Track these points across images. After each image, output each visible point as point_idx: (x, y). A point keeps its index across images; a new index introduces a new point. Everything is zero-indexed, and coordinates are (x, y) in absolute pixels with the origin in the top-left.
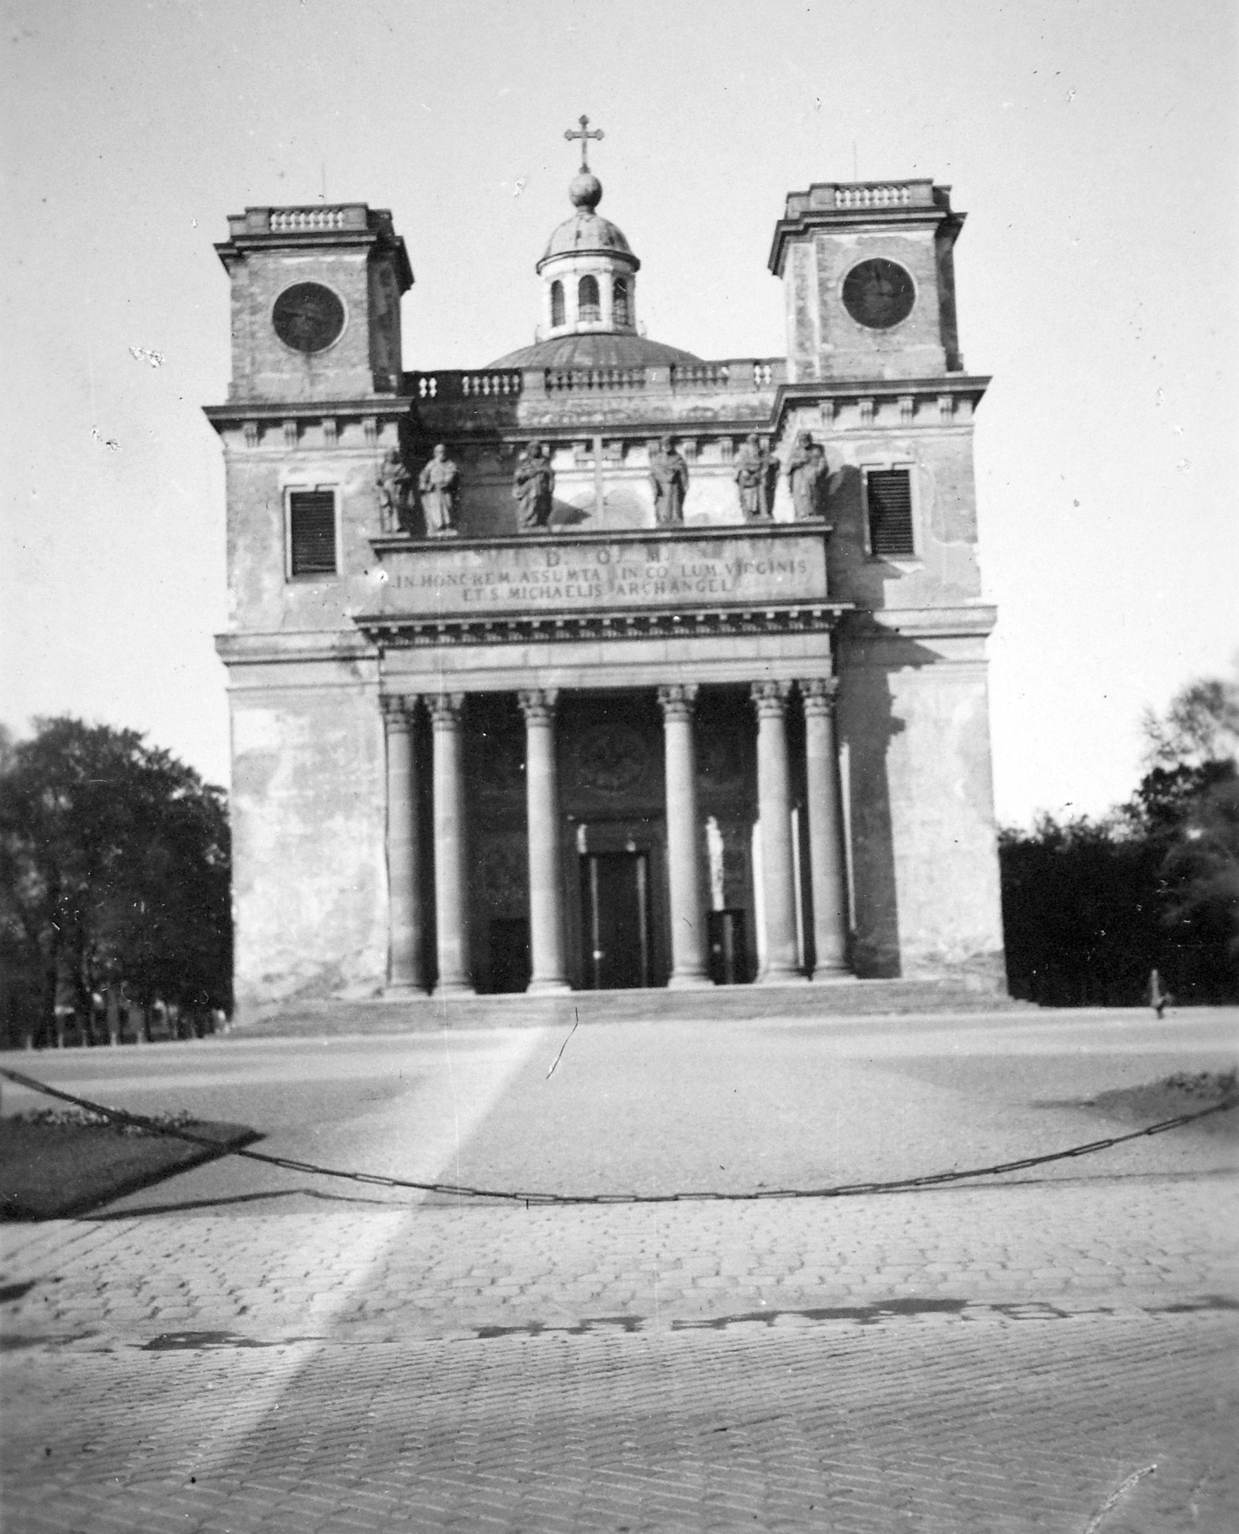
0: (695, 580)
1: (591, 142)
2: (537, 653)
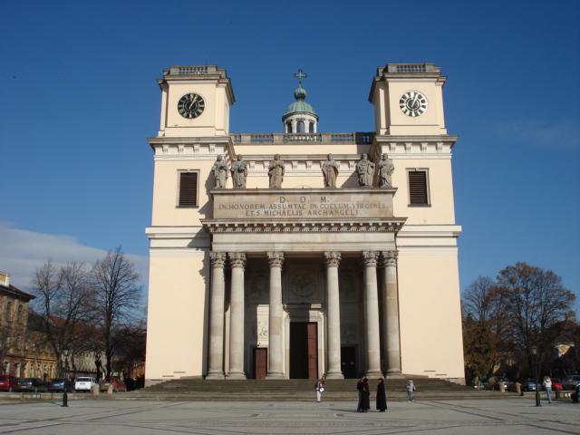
2: (274, 237)
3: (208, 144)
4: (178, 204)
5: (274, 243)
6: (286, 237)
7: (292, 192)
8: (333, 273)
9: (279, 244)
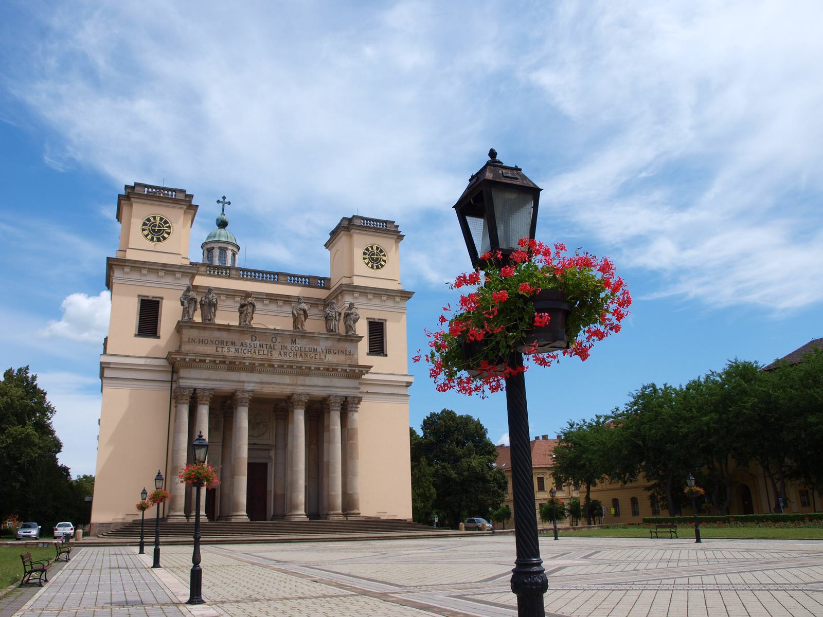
1: (226, 205)
2: (243, 376)
3: (175, 271)
4: (137, 333)
5: (244, 382)
6: (256, 377)
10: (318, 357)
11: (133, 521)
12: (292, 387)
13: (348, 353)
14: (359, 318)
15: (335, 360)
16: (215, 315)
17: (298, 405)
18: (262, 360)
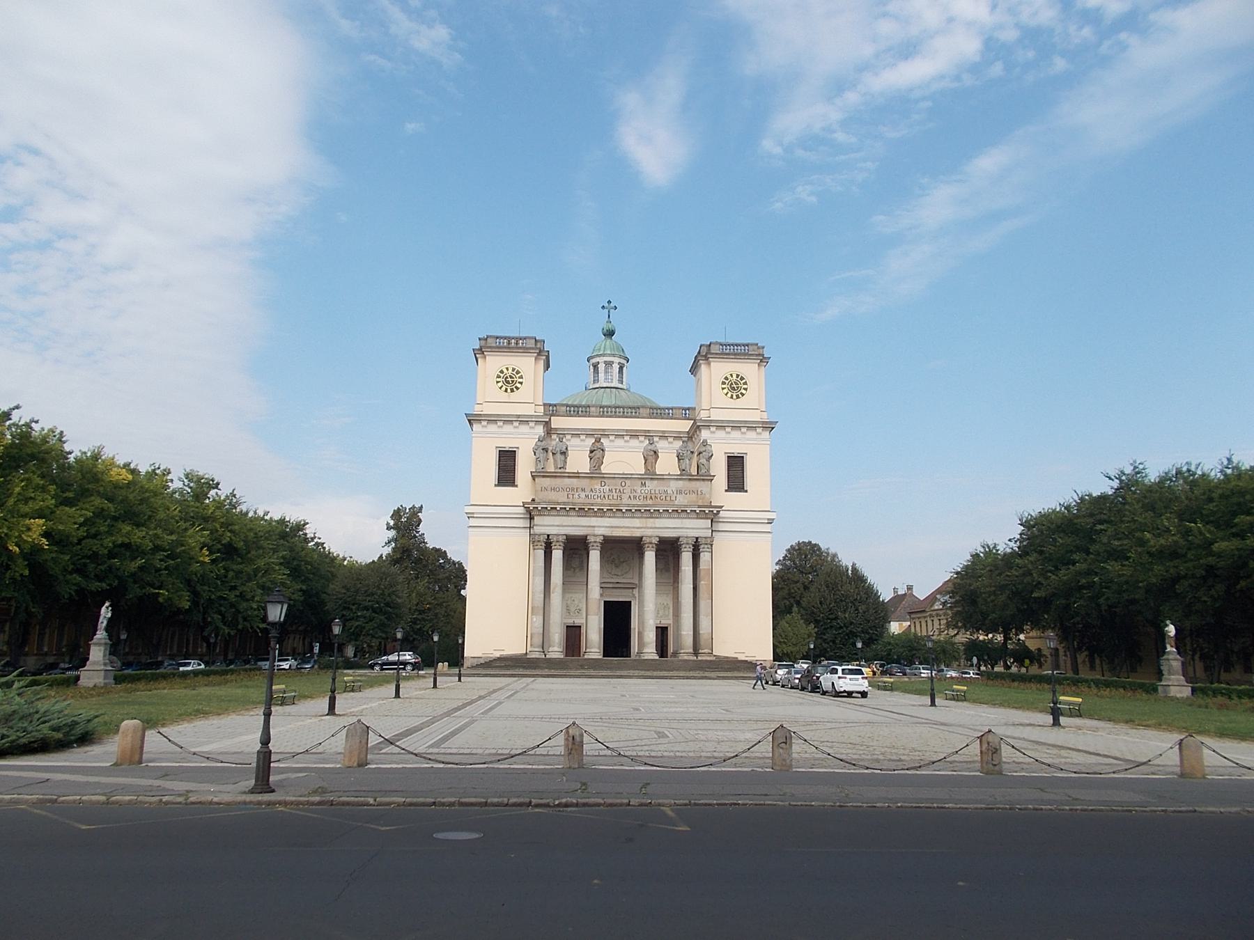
0: (659, 495)
1: (612, 311)
2: (594, 521)
4: (497, 483)
5: (594, 527)
7: (613, 477)
8: (650, 557)
9: (599, 527)
10: (668, 498)
11: (501, 655)
12: (643, 530)
13: (699, 493)
14: (712, 455)
15: (686, 501)
16: (566, 462)
17: (648, 547)
18: (610, 505)
